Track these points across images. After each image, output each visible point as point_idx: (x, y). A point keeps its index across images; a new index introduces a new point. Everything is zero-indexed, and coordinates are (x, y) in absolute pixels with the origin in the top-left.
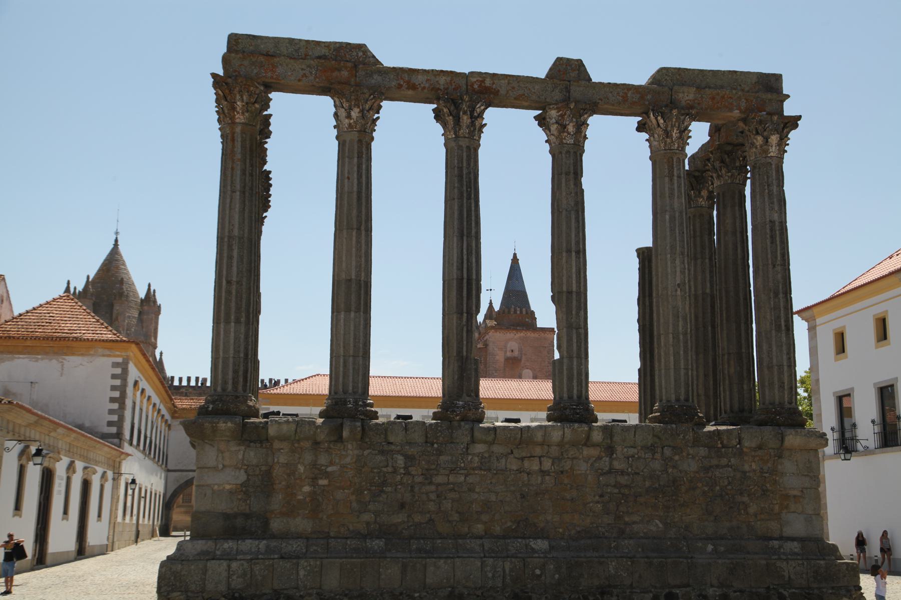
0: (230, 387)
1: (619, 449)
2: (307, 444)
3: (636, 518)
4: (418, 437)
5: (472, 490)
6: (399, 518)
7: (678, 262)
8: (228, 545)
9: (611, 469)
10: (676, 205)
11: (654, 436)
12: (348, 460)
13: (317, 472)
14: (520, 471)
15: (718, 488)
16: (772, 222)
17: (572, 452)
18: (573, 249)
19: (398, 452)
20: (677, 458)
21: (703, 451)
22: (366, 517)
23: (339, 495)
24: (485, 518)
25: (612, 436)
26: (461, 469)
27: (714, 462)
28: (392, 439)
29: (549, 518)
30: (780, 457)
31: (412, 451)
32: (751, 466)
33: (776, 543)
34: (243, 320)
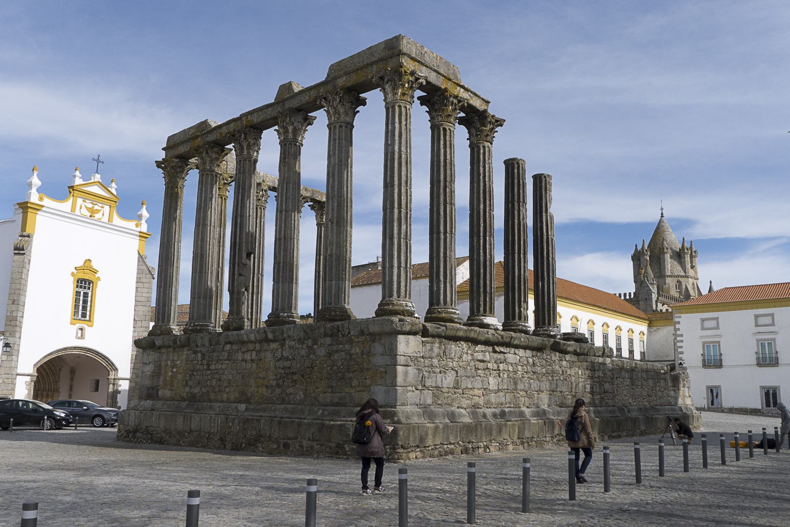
3: (291, 390)
5: (223, 374)
6: (196, 390)
14: (243, 360)
15: (335, 368)
17: (265, 345)
20: (315, 347)
21: (328, 340)
22: (187, 389)
24: (227, 390)
25: (282, 334)
27: (335, 348)
28: (199, 345)
29: (253, 389)
30: (374, 341)
31: (204, 350)
32: (357, 350)
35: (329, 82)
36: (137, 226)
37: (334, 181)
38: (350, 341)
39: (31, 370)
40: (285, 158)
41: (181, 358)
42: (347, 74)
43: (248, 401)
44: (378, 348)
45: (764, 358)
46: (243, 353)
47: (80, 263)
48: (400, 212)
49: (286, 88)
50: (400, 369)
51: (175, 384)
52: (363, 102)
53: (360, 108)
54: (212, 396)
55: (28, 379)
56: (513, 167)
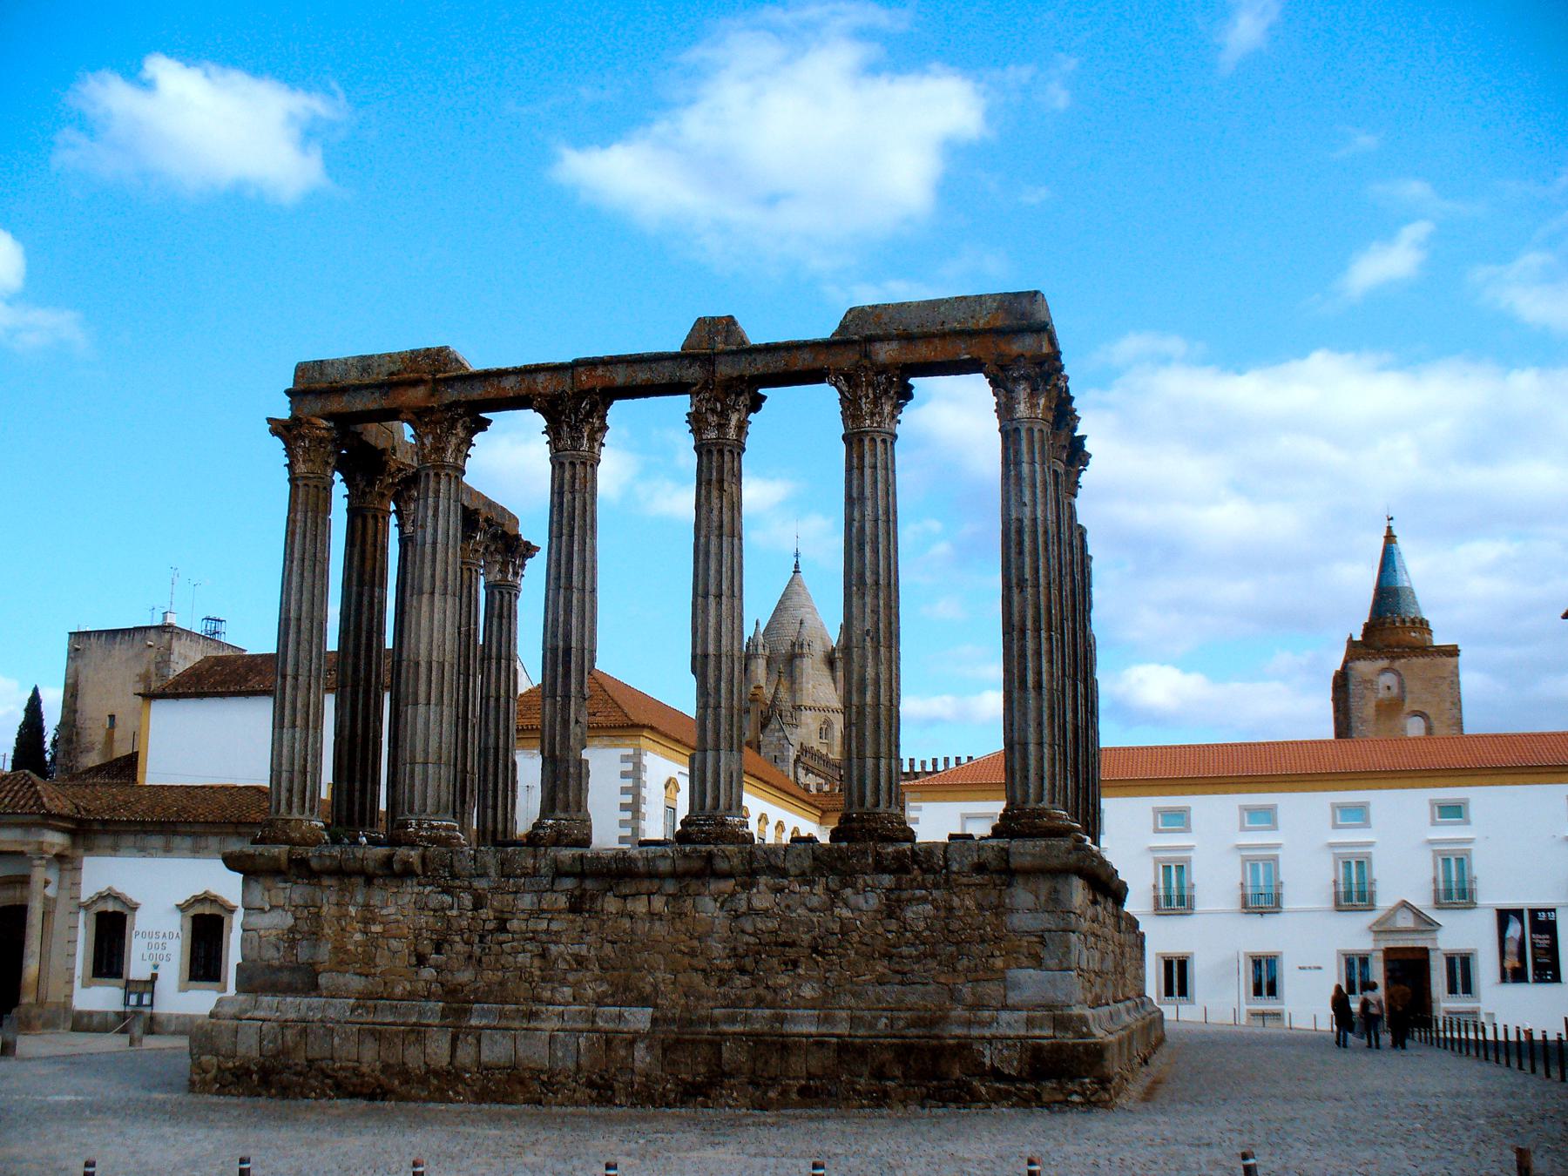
0: (283, 808)
1: (763, 880)
2: (361, 880)
5: (556, 943)
6: (465, 976)
7: (868, 599)
9: (750, 908)
11: (815, 859)
12: (406, 900)
14: (622, 914)
17: (694, 886)
18: (713, 589)
19: (465, 890)
20: (849, 891)
21: (887, 880)
22: (428, 973)
23: (394, 943)
24: (571, 977)
25: (750, 863)
26: (543, 911)
30: (1009, 885)
31: (481, 884)
33: (986, 1013)
34: (298, 722)
35: (854, 342)
38: (949, 885)
42: (907, 338)
43: (643, 1001)
44: (1022, 896)
46: (625, 897)
48: (1050, 638)
51: (382, 962)
52: (906, 394)
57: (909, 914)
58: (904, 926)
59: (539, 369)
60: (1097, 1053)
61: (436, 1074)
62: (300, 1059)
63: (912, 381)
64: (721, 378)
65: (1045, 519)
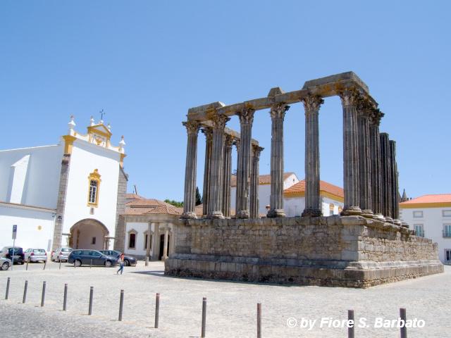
1: (284, 226)
2: (199, 227)
4: (226, 224)
6: (220, 250)
8: (180, 255)
10: (310, 133)
13: (201, 235)
16: (346, 132)
17: (269, 228)
21: (313, 227)
22: (213, 249)
23: (207, 242)
24: (242, 250)
27: (317, 230)
30: (343, 228)
31: (223, 228)
33: (335, 262)
36: (119, 150)
37: (311, 143)
39: (69, 232)
40: (276, 128)
41: (208, 232)
45: (447, 234)
47: (93, 172)
49: (275, 91)
50: (359, 242)
51: (203, 246)
53: (321, 105)
54: (231, 253)
55: (67, 237)
56: (384, 136)
57: (318, 235)
58: (316, 239)
59: (236, 105)
60: (362, 274)
61: (212, 272)
62: (185, 268)
63: (323, 99)
64: (278, 103)
65: (353, 131)
